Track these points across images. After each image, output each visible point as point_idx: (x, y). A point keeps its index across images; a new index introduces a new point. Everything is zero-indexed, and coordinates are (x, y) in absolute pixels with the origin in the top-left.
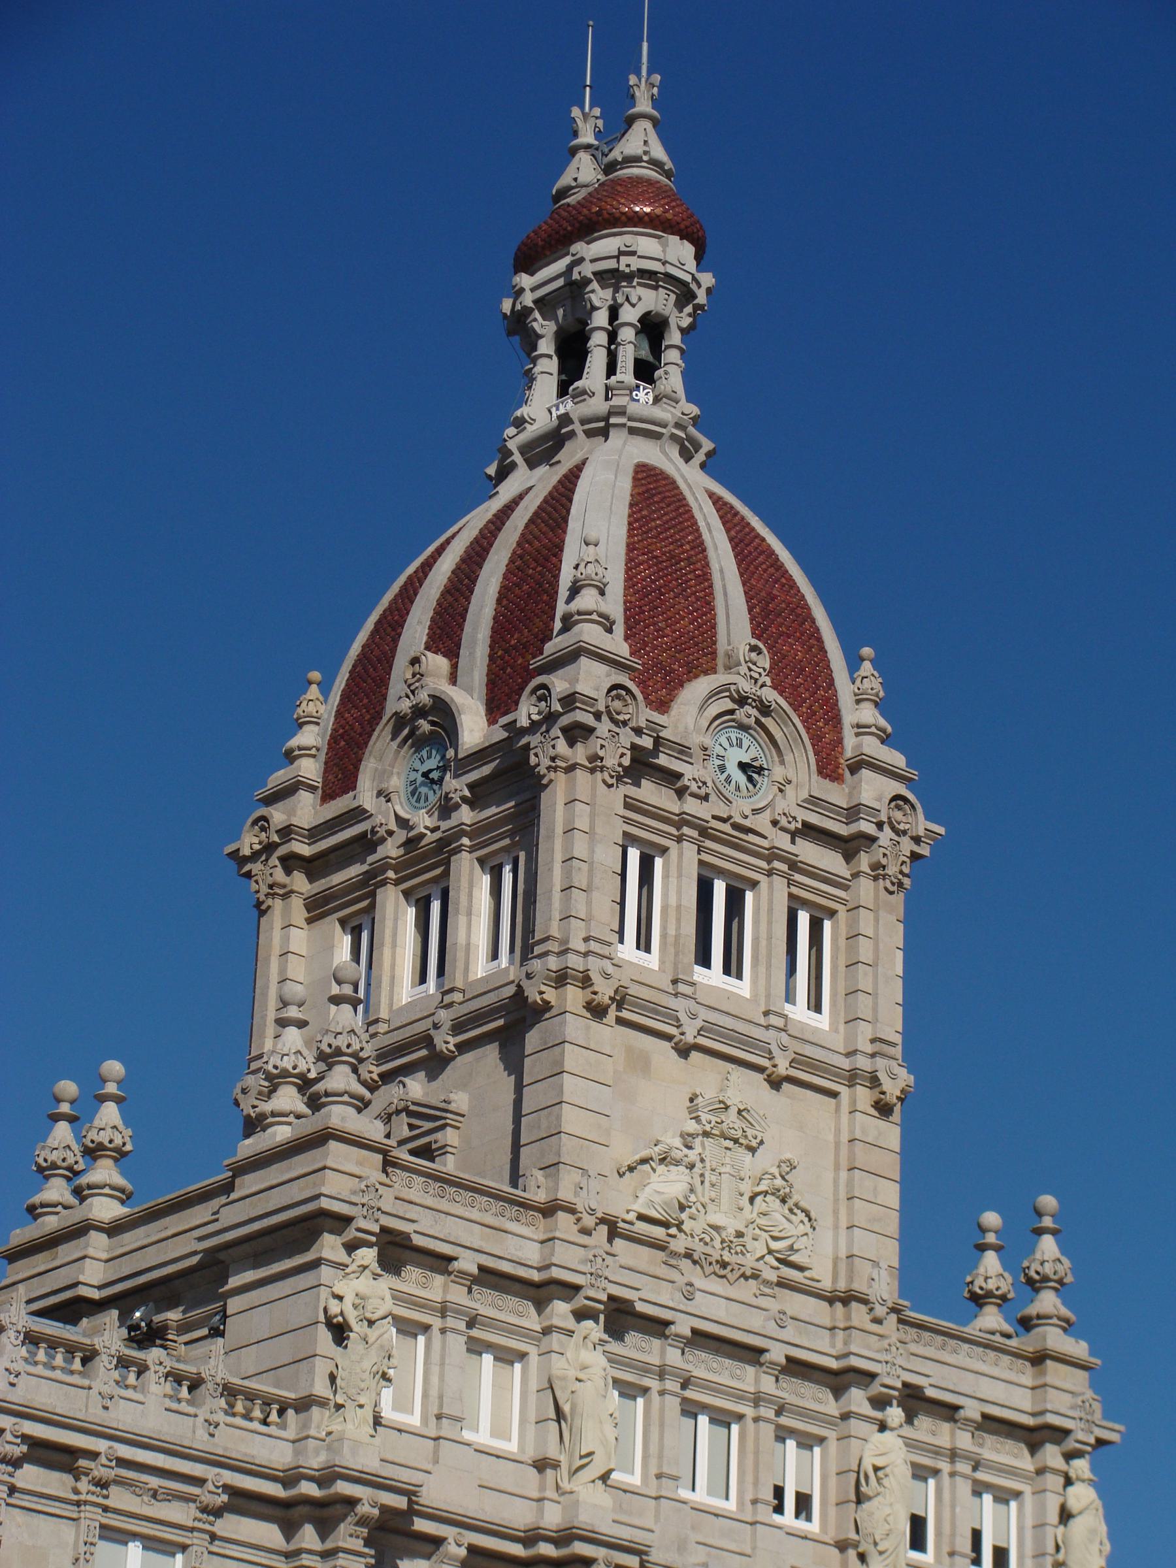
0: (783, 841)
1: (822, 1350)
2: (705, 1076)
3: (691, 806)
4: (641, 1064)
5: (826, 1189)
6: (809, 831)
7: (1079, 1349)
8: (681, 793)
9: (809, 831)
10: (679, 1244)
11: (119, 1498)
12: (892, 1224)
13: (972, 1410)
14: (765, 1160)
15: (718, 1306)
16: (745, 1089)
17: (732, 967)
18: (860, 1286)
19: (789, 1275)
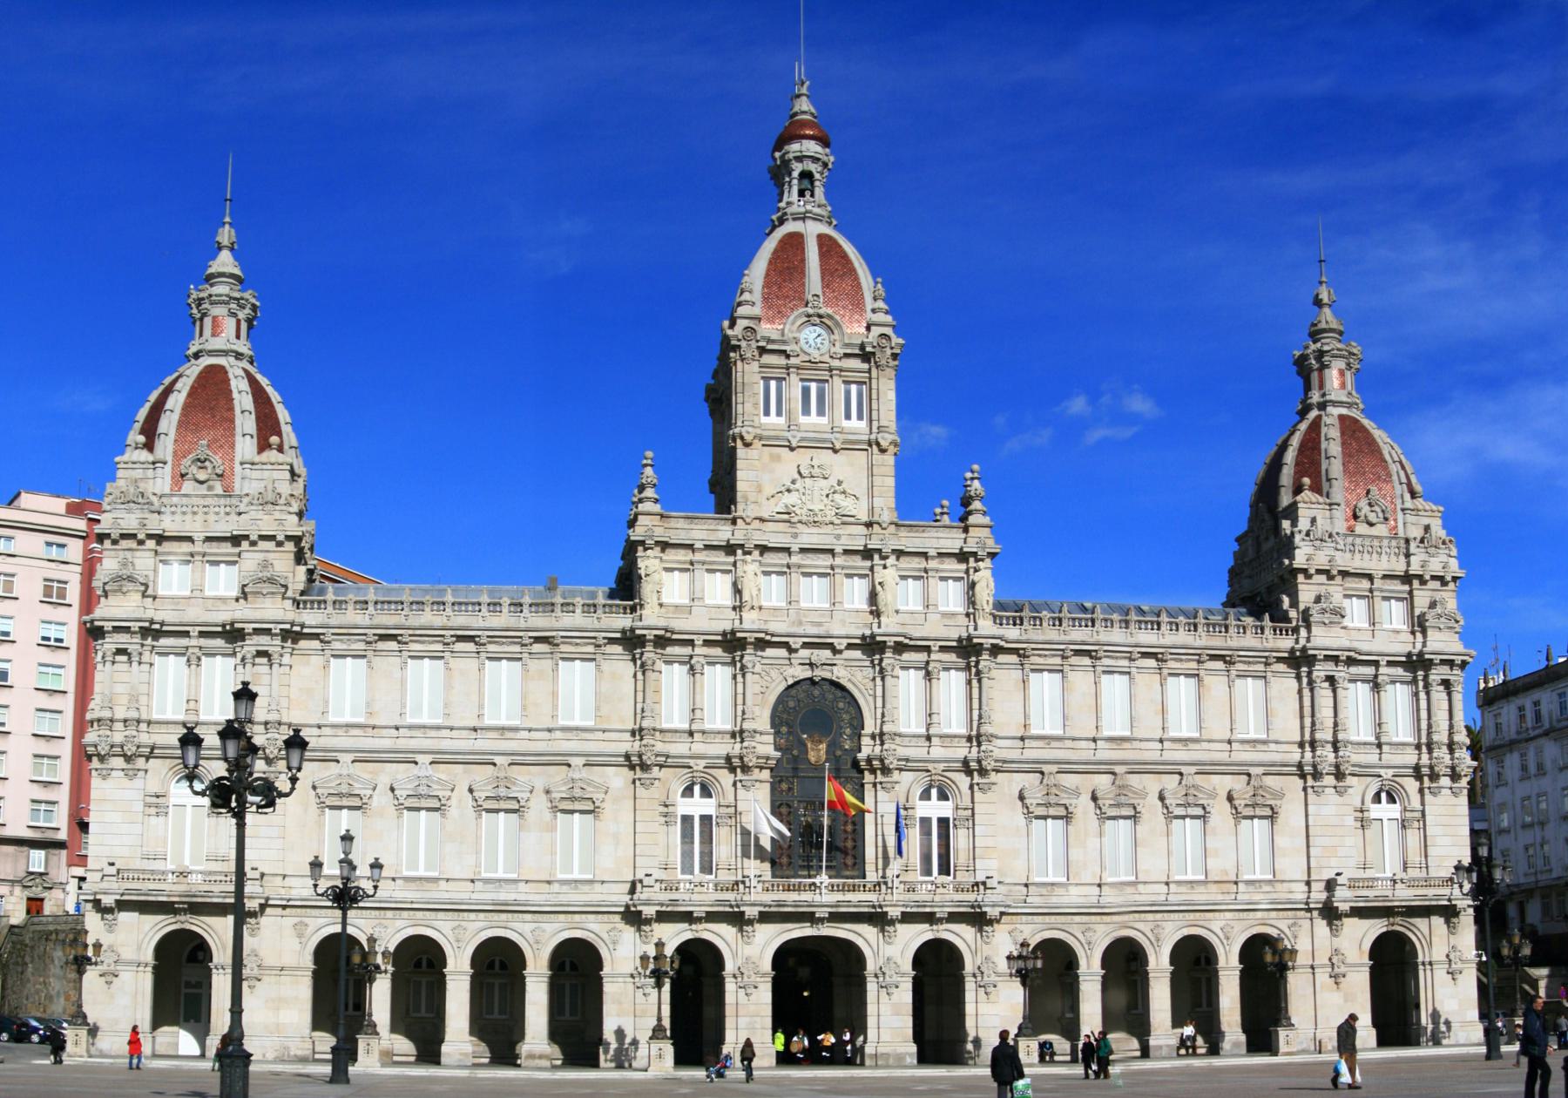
0: (836, 363)
1: (858, 544)
2: (803, 457)
3: (793, 361)
4: (777, 458)
5: (862, 486)
6: (847, 355)
7: (986, 520)
8: (788, 357)
9: (847, 355)
10: (795, 520)
11: (563, 648)
12: (892, 494)
13: (932, 553)
14: (833, 481)
15: (810, 537)
16: (825, 457)
17: (821, 412)
18: (876, 518)
19: (845, 519)
